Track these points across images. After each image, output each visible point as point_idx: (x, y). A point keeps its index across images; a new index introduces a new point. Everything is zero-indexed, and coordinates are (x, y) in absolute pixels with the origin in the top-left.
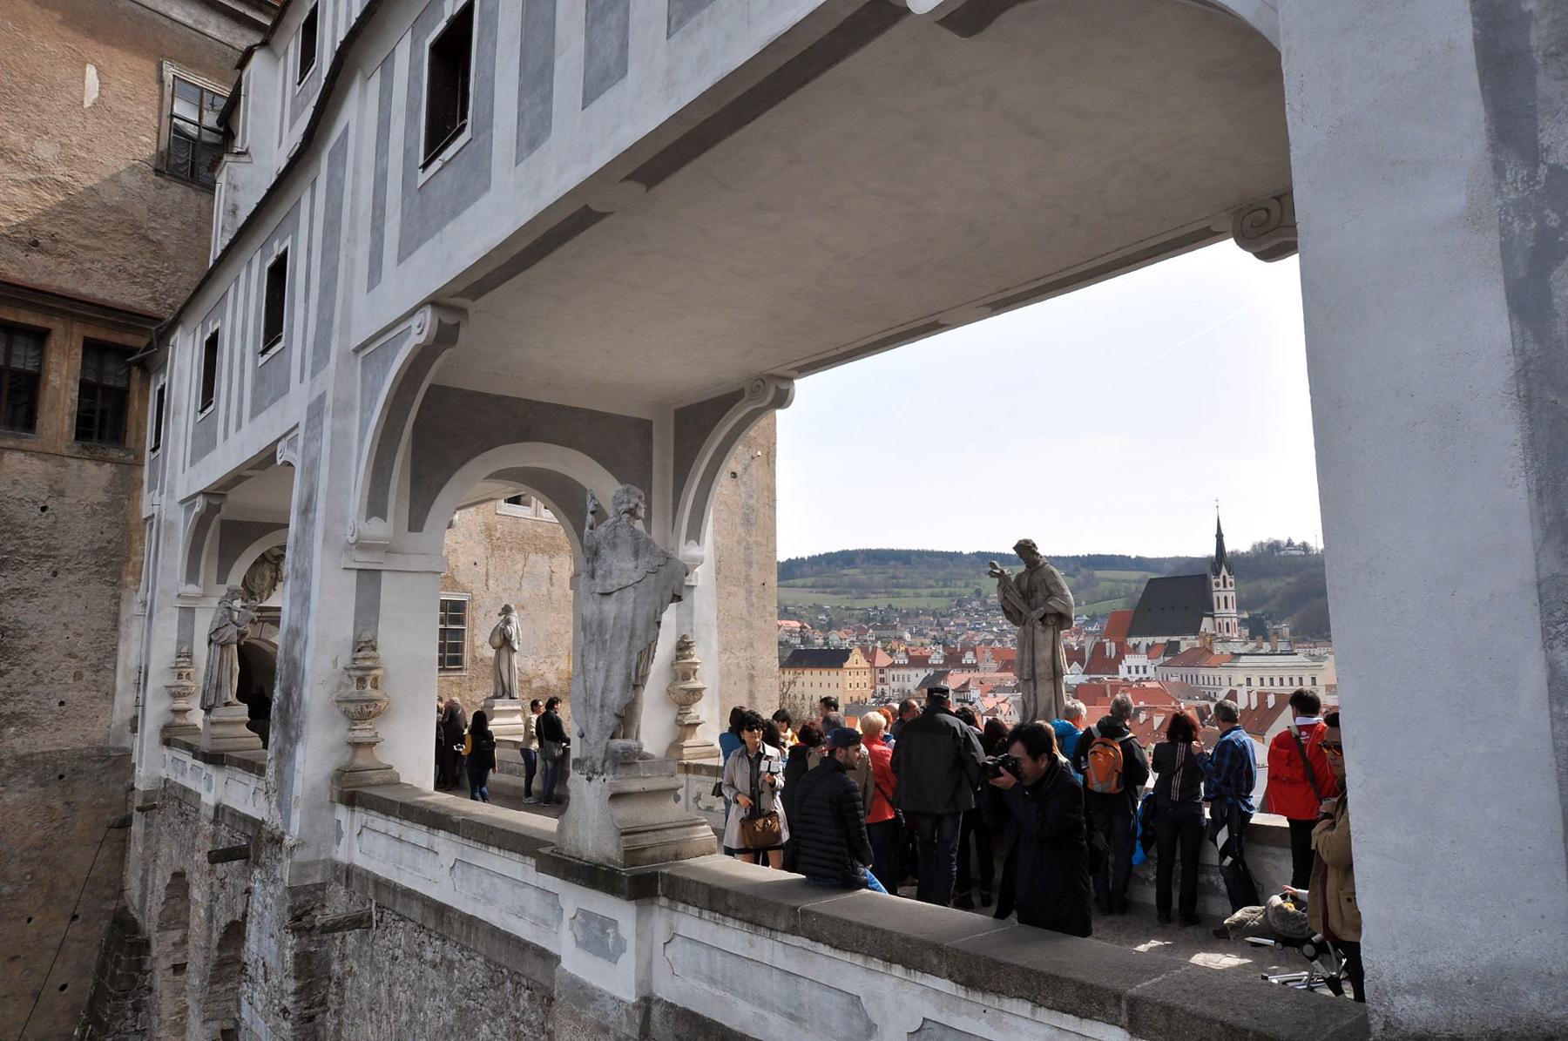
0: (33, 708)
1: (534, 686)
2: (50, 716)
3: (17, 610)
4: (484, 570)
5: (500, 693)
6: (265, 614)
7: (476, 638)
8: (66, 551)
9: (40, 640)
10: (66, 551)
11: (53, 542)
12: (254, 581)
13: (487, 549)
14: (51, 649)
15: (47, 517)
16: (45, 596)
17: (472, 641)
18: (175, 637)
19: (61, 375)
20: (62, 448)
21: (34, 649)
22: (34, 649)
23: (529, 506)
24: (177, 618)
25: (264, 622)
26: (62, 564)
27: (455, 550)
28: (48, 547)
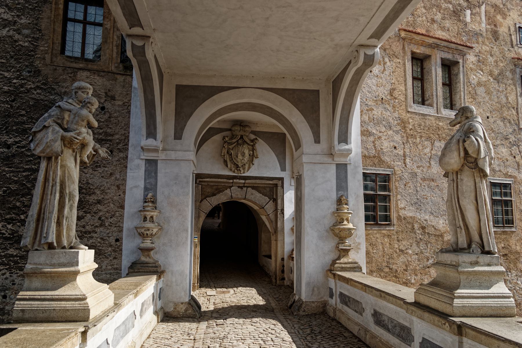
0: (99, 242)
1: (446, 239)
2: (110, 249)
3: (88, 175)
4: (401, 153)
5: (463, 241)
6: (247, 181)
7: (399, 202)
8: (117, 136)
9: (103, 196)
10: (117, 136)
11: (109, 131)
12: (237, 157)
13: (403, 137)
14: (109, 202)
15: (104, 114)
16: (106, 167)
17: (397, 204)
18: (142, 184)
19: (110, 20)
20: (113, 68)
21: (99, 202)
22: (99, 202)
23: (431, 105)
24: (143, 169)
25: (247, 187)
26: (115, 145)
27: (380, 138)
28: (106, 134)
